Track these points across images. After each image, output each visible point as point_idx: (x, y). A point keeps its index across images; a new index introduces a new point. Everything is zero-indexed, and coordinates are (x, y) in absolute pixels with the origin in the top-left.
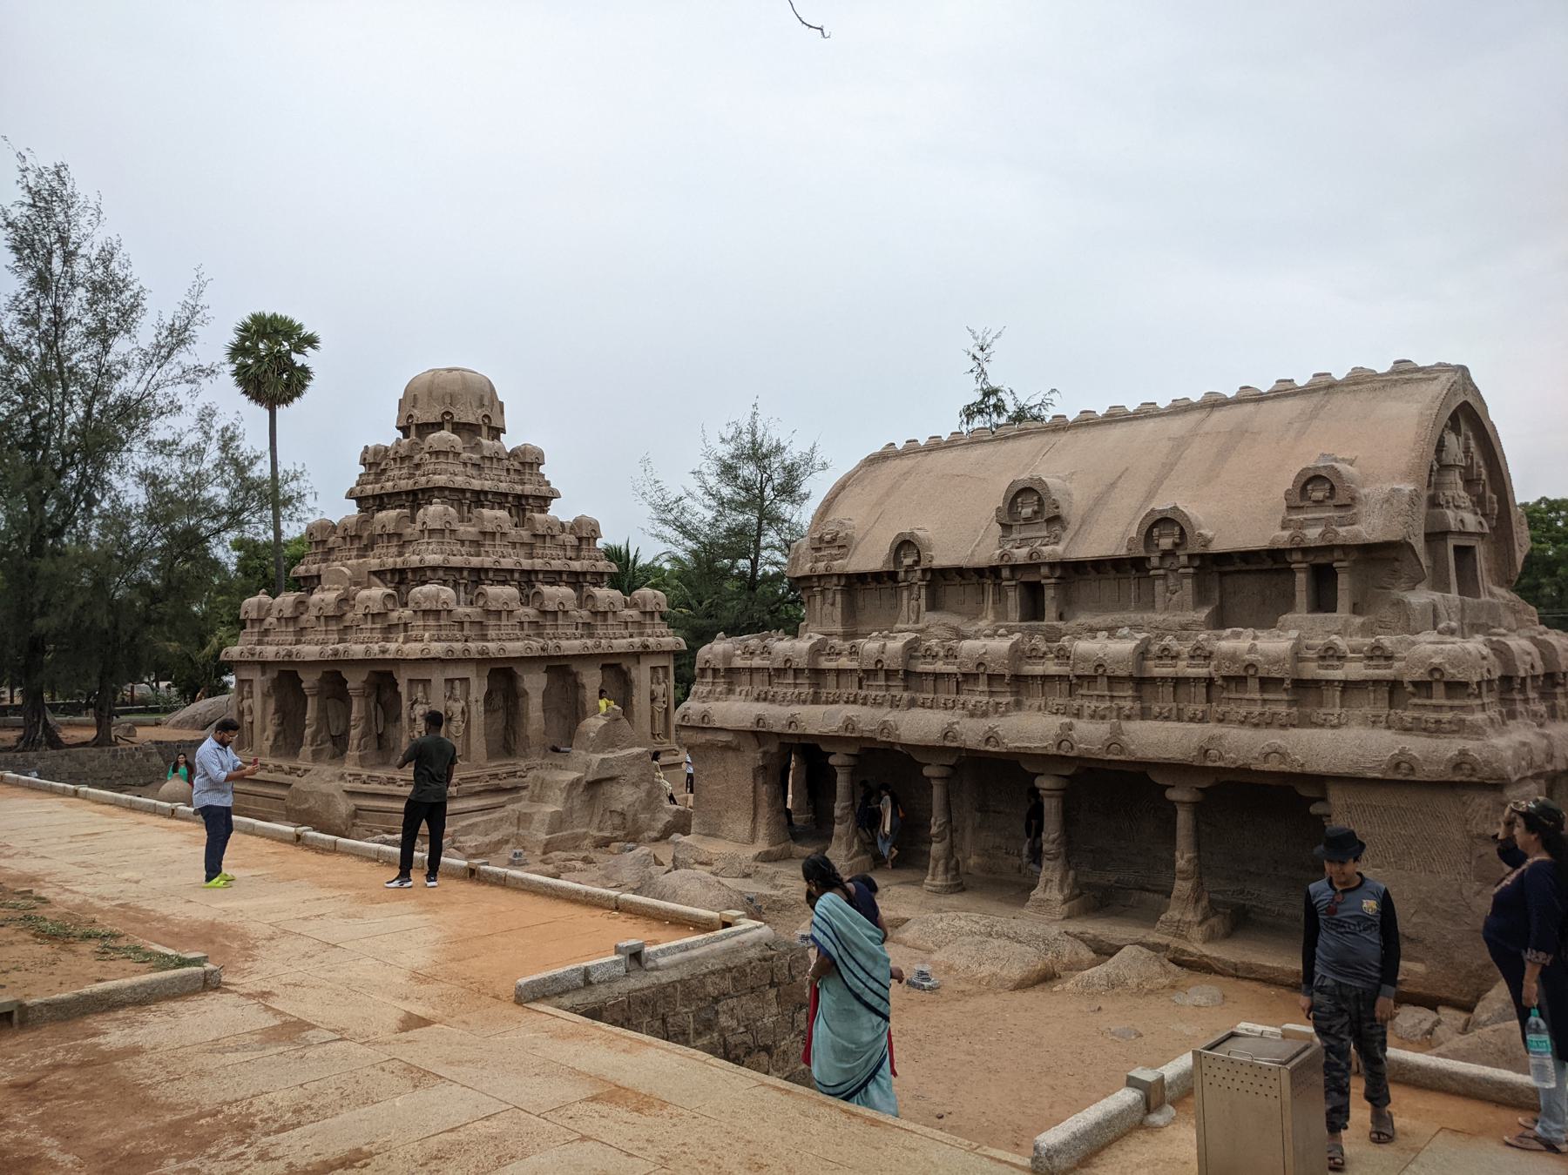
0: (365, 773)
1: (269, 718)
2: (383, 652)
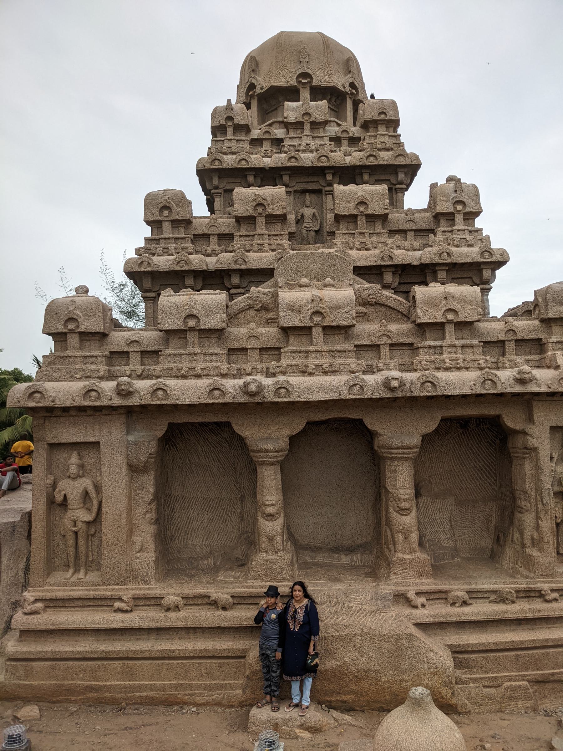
0: (459, 589)
1: (140, 510)
2: (521, 381)
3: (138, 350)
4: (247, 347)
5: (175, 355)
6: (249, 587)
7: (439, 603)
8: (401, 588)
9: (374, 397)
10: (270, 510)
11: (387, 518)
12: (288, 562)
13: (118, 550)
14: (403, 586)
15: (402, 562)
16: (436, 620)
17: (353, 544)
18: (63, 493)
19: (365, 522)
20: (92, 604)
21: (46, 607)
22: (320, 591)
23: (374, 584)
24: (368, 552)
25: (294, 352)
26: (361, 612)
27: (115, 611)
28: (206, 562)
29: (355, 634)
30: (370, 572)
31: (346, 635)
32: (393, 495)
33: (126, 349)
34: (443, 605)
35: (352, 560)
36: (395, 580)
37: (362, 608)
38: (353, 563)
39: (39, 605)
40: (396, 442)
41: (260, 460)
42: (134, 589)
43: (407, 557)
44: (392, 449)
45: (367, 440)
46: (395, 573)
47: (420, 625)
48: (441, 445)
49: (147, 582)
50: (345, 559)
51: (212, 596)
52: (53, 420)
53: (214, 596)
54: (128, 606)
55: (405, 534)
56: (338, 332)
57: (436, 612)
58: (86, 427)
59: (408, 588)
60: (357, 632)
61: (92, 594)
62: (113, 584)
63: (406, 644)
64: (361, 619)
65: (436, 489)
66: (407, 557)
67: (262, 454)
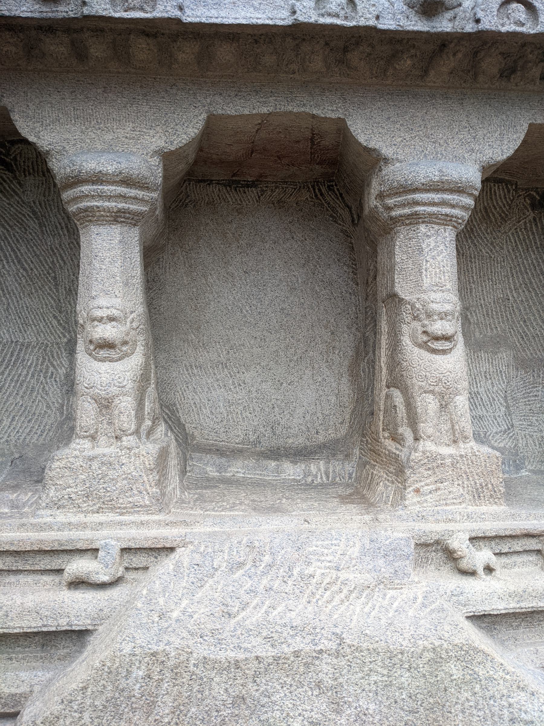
6: (41, 528)
7: (524, 564)
8: (433, 528)
9: (380, 26)
11: (395, 363)
12: (150, 461)
14: (437, 521)
15: (434, 463)
16: (523, 605)
17: (308, 444)
19: (333, 399)
22: (229, 536)
23: (367, 518)
24: (341, 457)
26: (335, 588)
29: (321, 652)
30: (351, 495)
31: (297, 654)
32: (413, 306)
34: (531, 568)
35: (307, 474)
36: (417, 508)
37: (337, 578)
38: (310, 479)
40: (426, 171)
43: (445, 451)
44: (416, 190)
45: (342, 231)
46: (417, 491)
47: (484, 620)
48: (492, 244)
50: (292, 471)
55: (442, 395)
57: (523, 586)
59: (451, 526)
60: (325, 644)
63: (457, 674)
64: (336, 608)
65: (477, 334)
66: (445, 451)
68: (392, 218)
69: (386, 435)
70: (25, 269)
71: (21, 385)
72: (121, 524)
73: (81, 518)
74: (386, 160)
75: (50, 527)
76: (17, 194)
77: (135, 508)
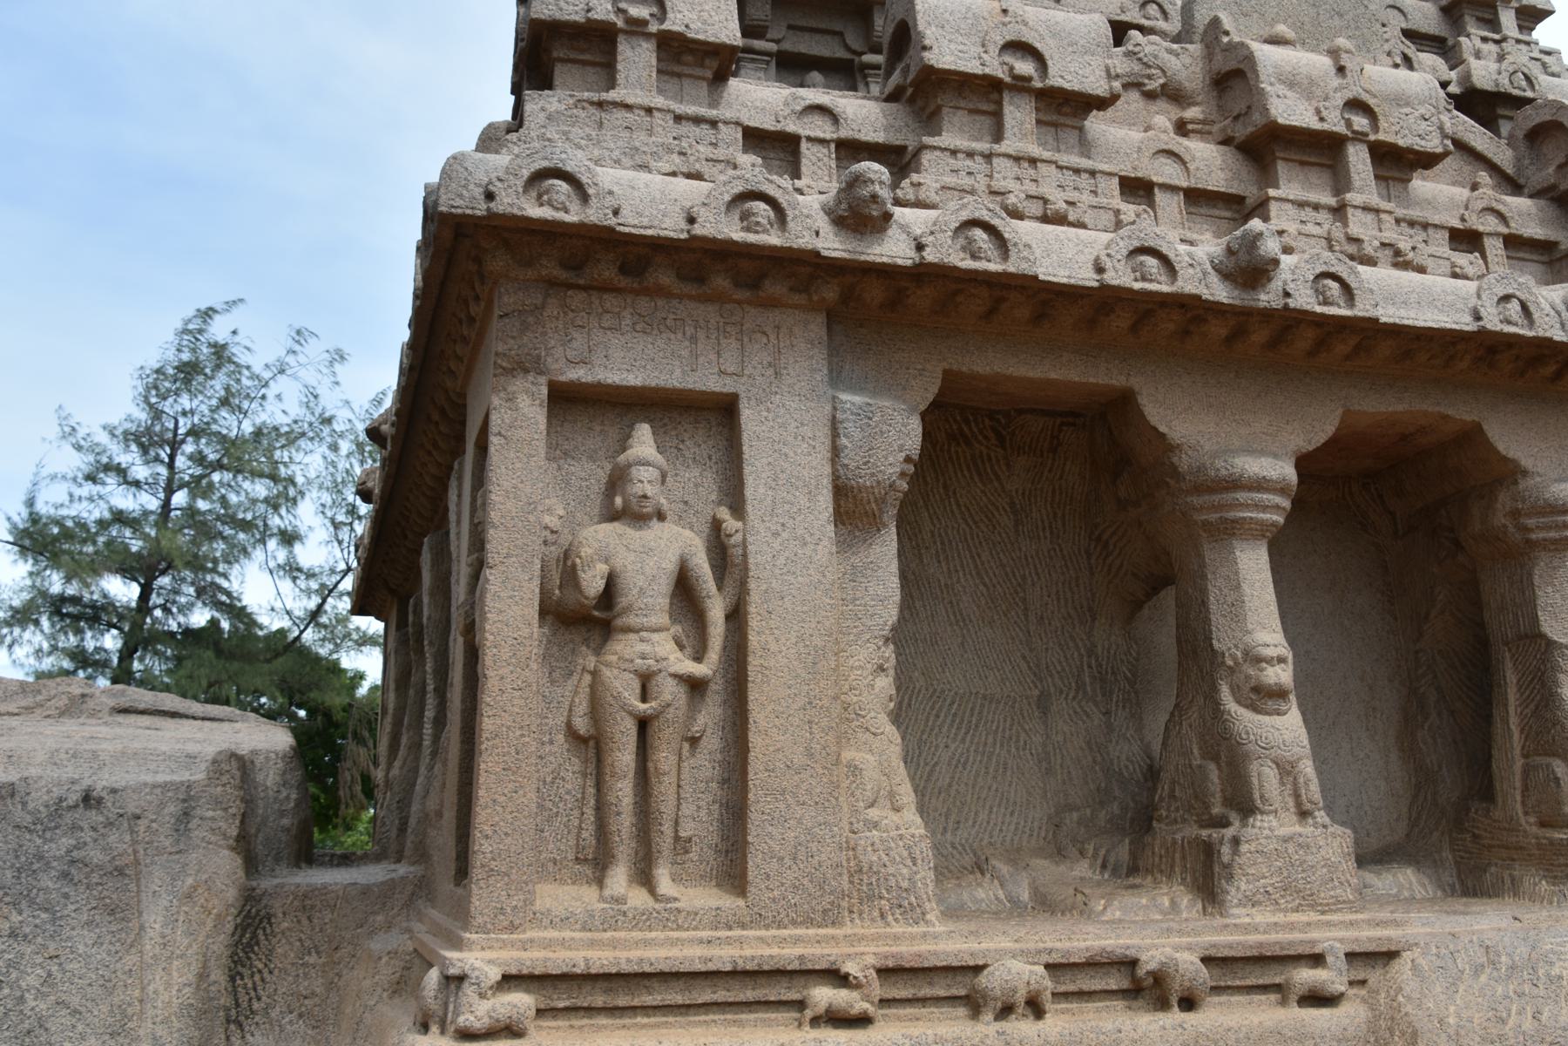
3: (828, 136)
4: (1155, 179)
5: (970, 154)
10: (1281, 675)
13: (809, 792)
18: (602, 568)
20: (721, 995)
21: (538, 1011)
25: (1301, 205)
27: (816, 1021)
28: (981, 894)
33: (791, 127)
39: (521, 1001)
41: (1232, 515)
42: (876, 938)
49: (913, 913)
51: (1143, 958)
52: (577, 298)
53: (1151, 960)
54: (866, 998)
56: (1397, 174)
58: (694, 339)
61: (724, 956)
62: (794, 923)
67: (1242, 496)
68: (1528, 541)
69: (1532, 820)
70: (985, 585)
71: (990, 759)
72: (1329, 924)
73: (1279, 918)
74: (1525, 473)
75: (1246, 929)
76: (998, 478)
77: (1337, 905)
